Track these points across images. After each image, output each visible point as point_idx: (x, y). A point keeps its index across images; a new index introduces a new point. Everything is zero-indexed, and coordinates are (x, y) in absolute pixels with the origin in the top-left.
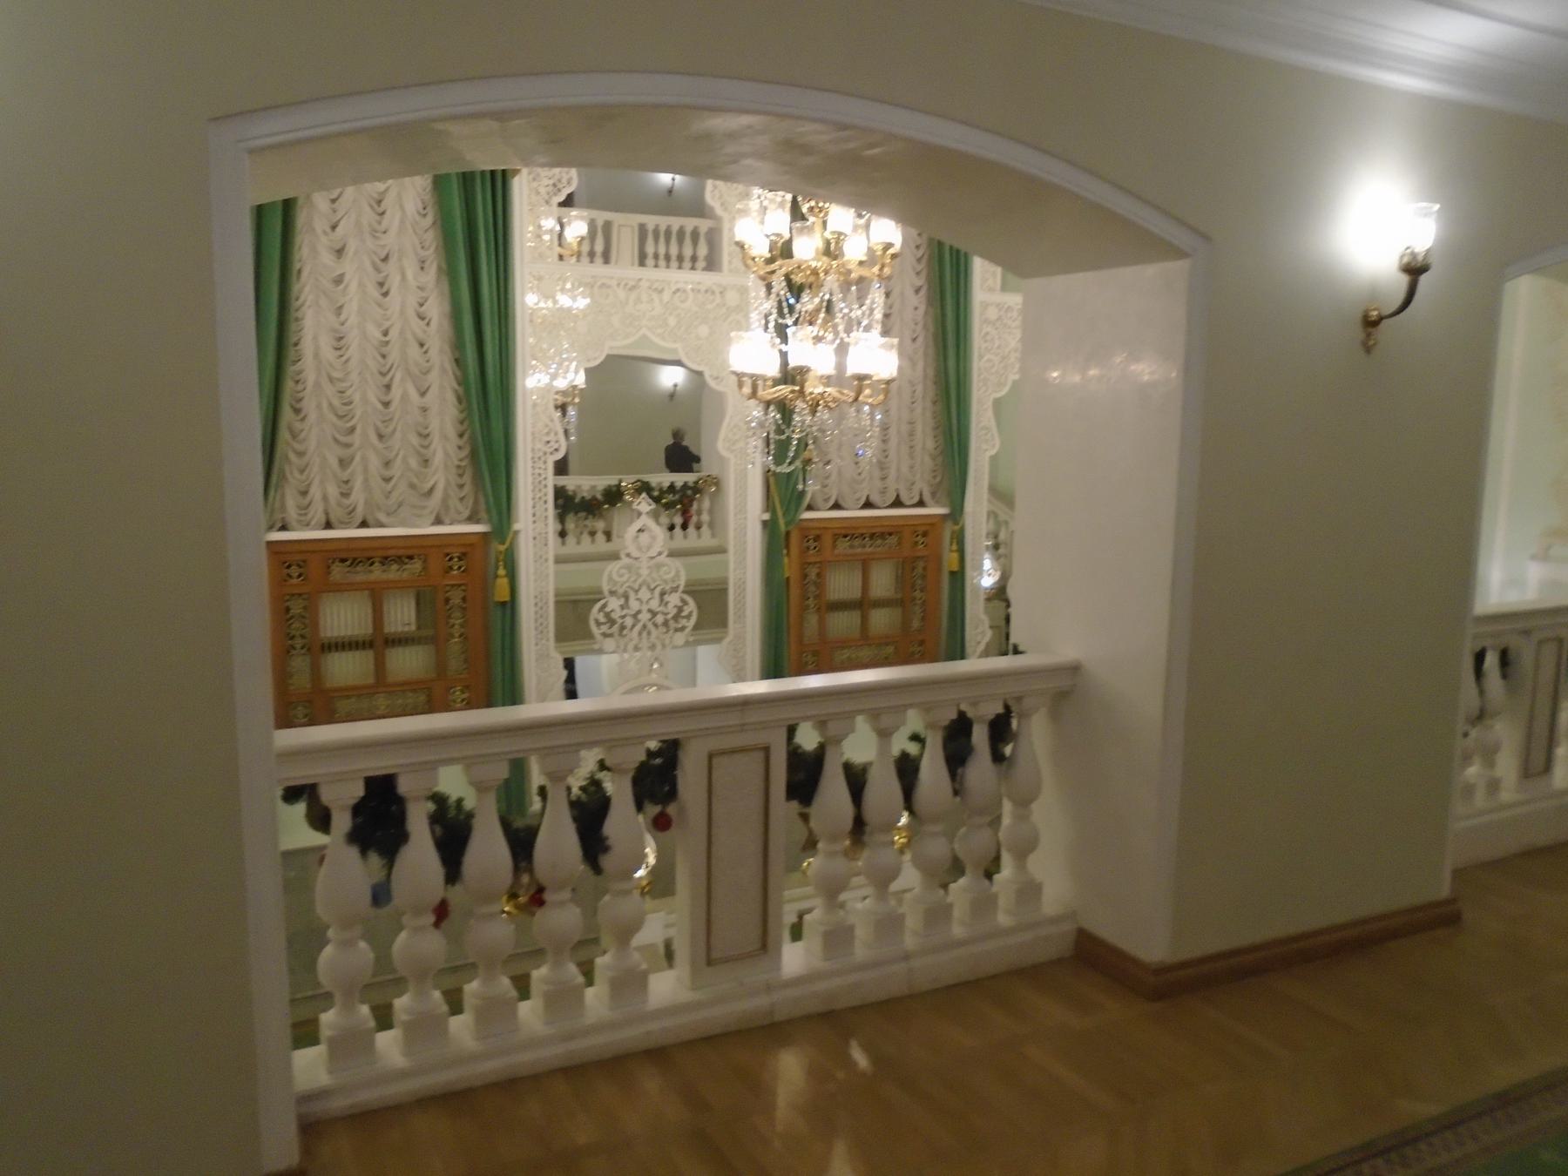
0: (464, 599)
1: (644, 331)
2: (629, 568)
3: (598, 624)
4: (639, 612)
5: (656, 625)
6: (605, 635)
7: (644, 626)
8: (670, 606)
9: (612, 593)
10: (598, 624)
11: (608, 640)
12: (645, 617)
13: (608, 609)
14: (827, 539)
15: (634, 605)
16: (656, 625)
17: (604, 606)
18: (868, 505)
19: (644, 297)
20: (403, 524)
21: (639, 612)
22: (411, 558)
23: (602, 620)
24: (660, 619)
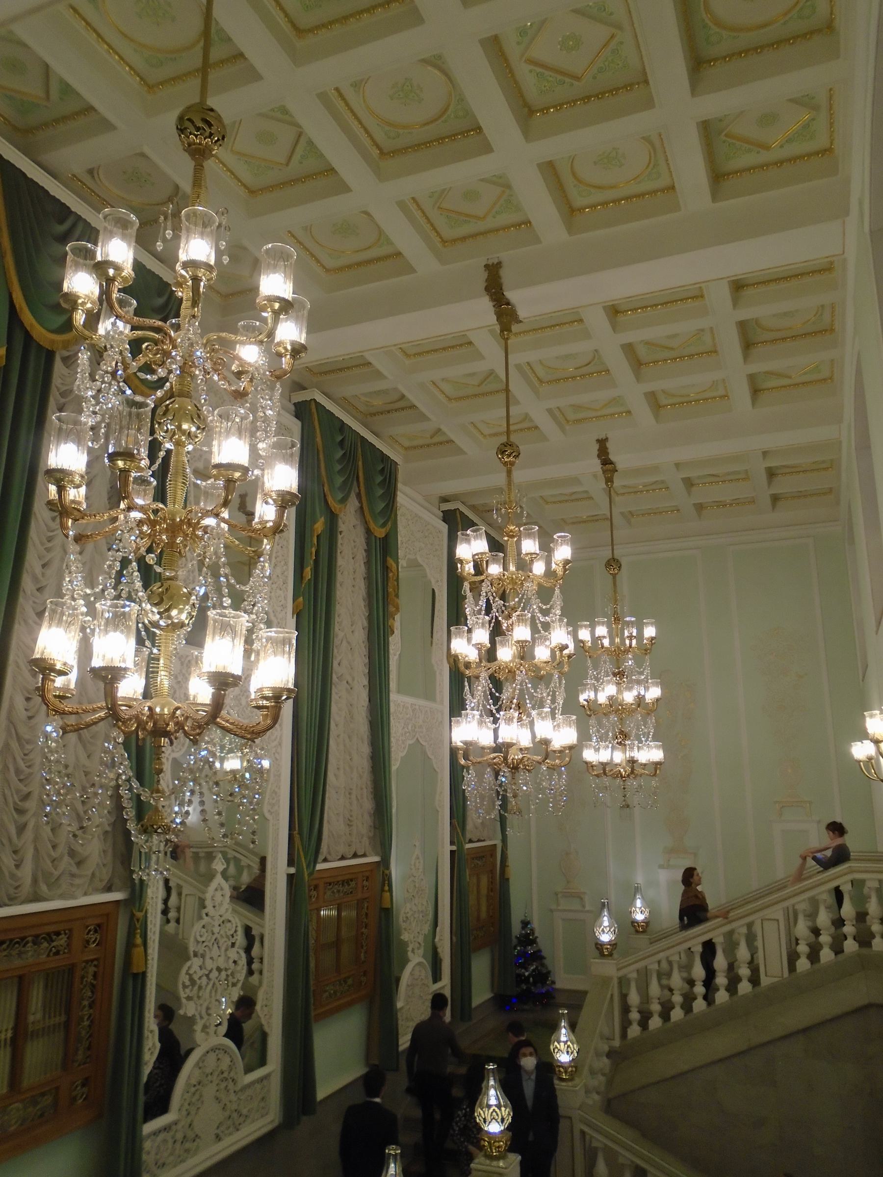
0: (95, 975)
4: (211, 971)
6: (189, 998)
7: (214, 984)
9: (196, 955)
10: (185, 987)
11: (191, 1003)
15: (209, 964)
17: (189, 968)
18: (343, 858)
20: (62, 897)
22: (58, 934)
23: (188, 983)
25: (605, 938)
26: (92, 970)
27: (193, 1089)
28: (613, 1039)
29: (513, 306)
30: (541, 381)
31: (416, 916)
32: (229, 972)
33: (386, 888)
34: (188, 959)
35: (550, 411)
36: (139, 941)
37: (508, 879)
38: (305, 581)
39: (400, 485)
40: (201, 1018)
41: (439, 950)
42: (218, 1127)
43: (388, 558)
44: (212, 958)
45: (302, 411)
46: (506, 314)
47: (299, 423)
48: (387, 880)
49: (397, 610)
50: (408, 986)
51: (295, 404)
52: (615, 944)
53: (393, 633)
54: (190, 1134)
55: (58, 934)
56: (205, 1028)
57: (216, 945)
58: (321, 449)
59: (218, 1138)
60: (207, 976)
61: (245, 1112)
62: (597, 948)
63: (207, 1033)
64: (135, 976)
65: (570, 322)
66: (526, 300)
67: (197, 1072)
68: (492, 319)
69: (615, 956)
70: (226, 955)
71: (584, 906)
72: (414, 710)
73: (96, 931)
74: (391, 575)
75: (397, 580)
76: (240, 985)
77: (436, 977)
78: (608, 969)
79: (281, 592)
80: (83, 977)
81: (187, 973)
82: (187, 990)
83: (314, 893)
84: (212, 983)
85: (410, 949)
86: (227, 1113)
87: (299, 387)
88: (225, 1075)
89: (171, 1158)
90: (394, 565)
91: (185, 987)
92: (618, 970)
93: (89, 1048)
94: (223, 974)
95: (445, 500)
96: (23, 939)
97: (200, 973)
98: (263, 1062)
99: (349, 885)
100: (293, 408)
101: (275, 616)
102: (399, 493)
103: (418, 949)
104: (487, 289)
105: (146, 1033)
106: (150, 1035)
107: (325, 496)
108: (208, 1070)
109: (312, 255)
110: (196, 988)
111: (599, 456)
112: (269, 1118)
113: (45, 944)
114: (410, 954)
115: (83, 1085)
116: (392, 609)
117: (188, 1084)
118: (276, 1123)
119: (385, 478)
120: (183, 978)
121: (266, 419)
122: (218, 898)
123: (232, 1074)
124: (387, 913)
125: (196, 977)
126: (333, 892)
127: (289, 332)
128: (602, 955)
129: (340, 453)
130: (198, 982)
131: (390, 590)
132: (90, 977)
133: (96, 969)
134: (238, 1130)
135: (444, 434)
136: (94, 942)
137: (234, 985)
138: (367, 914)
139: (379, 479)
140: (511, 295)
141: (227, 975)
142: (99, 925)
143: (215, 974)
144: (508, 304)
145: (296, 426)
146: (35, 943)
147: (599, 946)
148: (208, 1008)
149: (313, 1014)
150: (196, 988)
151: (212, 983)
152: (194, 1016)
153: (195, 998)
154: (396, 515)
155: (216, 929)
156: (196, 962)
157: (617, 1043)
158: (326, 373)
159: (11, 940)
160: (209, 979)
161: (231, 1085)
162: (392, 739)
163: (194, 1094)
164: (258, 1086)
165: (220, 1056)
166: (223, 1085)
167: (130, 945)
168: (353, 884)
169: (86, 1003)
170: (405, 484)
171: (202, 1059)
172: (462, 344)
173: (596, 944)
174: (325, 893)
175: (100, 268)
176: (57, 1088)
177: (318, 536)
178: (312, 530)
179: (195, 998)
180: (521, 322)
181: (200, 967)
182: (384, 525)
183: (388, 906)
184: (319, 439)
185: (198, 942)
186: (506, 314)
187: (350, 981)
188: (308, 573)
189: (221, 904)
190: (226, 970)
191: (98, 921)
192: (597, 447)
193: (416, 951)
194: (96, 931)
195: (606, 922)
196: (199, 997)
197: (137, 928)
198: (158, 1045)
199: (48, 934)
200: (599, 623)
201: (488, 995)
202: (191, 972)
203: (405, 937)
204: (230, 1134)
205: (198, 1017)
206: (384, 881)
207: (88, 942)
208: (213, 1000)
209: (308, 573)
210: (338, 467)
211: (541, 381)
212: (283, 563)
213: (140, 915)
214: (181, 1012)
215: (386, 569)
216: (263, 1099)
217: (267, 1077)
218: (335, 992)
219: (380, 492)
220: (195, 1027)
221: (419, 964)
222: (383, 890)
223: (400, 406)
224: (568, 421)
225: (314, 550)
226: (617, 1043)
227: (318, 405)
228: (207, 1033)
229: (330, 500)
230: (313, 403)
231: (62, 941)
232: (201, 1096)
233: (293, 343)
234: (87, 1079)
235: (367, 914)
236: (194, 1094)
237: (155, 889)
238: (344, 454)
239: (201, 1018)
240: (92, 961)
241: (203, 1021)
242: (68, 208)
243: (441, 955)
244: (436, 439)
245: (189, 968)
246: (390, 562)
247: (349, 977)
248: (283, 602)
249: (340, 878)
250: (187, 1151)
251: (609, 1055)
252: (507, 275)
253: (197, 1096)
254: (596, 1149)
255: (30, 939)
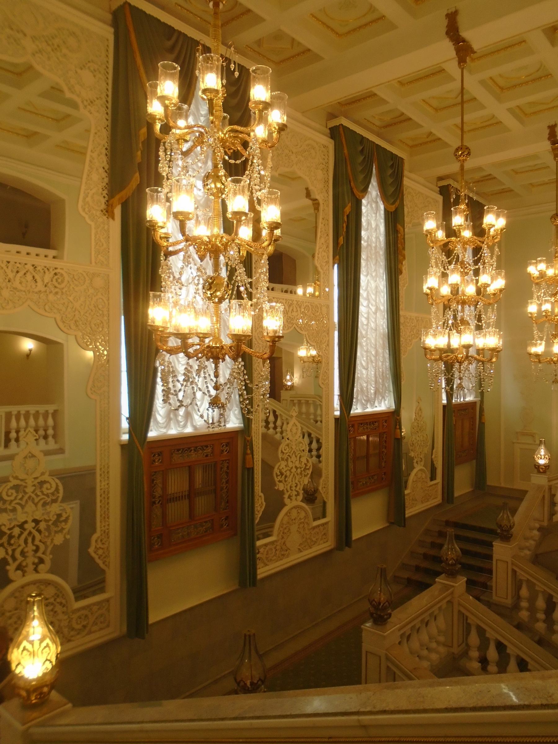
0: (228, 467)
1: (295, 325)
2: (288, 445)
3: (277, 476)
4: (292, 468)
5: (297, 474)
6: (280, 481)
7: (294, 475)
8: (303, 464)
9: (283, 459)
12: (294, 470)
13: (281, 468)
14: (356, 426)
15: (290, 465)
16: (297, 474)
17: (279, 466)
19: (295, 310)
21: (292, 468)
22: (207, 447)
23: (279, 474)
24: (299, 470)
25: (542, 462)
26: (226, 465)
27: (285, 526)
28: (543, 521)
29: (467, 42)
30: (502, 89)
31: (419, 443)
32: (302, 469)
33: (398, 427)
34: (279, 461)
35: (510, 110)
36: (249, 451)
37: (484, 423)
38: (340, 246)
39: (406, 173)
40: (287, 491)
41: (435, 463)
42: (299, 546)
43: (398, 224)
44: (292, 462)
45: (335, 133)
46: (463, 50)
47: (332, 142)
48: (398, 423)
49: (404, 258)
50: (413, 481)
51: (330, 129)
52: (549, 466)
53: (401, 273)
54: (284, 547)
55: (207, 447)
56: (290, 497)
57: (294, 455)
58: (347, 158)
59: (300, 551)
60: (290, 470)
61: (314, 539)
62: (536, 468)
63: (291, 500)
64: (249, 469)
65: (515, 46)
66: (477, 36)
67: (286, 519)
68: (453, 53)
69: (548, 473)
70: (300, 461)
71: (535, 441)
72: (417, 321)
73: (227, 446)
74: (399, 235)
75: (404, 239)
76: (309, 476)
77: (433, 478)
78: (541, 480)
79: (325, 254)
80: (222, 468)
81: (278, 468)
82: (279, 477)
83: (352, 429)
84: (292, 475)
85: (415, 461)
86: (304, 539)
87: (332, 116)
88: (303, 520)
89: (275, 557)
90: (402, 229)
91: (277, 476)
92: (549, 481)
93: (227, 502)
94: (299, 470)
95: (440, 179)
96: (189, 448)
97: (285, 469)
98: (324, 516)
99: (374, 425)
100: (329, 131)
101: (322, 268)
102: (405, 179)
103: (421, 461)
104: (447, 33)
105: (256, 498)
106: (260, 499)
107: (352, 189)
108: (293, 518)
109: (328, 27)
110: (284, 476)
111: (549, 139)
112: (329, 543)
113: (201, 451)
114: (415, 465)
115: (226, 519)
116: (401, 258)
117: (282, 524)
118: (332, 547)
119: (394, 171)
120: (276, 471)
121: (261, 178)
122: (294, 430)
123: (306, 521)
124: (399, 440)
125: (283, 471)
126: (364, 429)
127: (276, 117)
128: (539, 472)
129: (361, 158)
130: (285, 473)
131: (399, 245)
132: (225, 469)
133: (227, 464)
134: (311, 548)
135: (434, 135)
136: (226, 451)
137: (305, 476)
138: (386, 441)
139: (390, 171)
140: (465, 34)
141: (301, 471)
142: (228, 443)
143: (294, 470)
144: (464, 41)
145: (330, 144)
146: (195, 451)
147: (538, 467)
148: (291, 487)
149: (351, 494)
150: (284, 476)
151: (292, 475)
152: (283, 490)
153: (283, 481)
154: (403, 195)
155: (294, 447)
156: (283, 464)
157: (545, 523)
158: (349, 104)
159: (183, 449)
160: (291, 472)
161: (306, 526)
162: (401, 339)
163: (285, 528)
164: (321, 528)
165: (299, 511)
166: (301, 526)
167: (245, 454)
168: (376, 424)
169: (224, 481)
170: (410, 171)
171: (289, 512)
172: (438, 72)
173: (535, 465)
174: (358, 429)
175: (162, 99)
176: (212, 520)
177: (348, 216)
178: (343, 212)
179: (283, 481)
180: (475, 52)
181: (286, 466)
182: (393, 203)
183: (399, 437)
184: (346, 151)
185: (283, 453)
186: (463, 50)
187: (376, 477)
188: (341, 240)
189: (296, 433)
190: (301, 468)
191: (227, 441)
192: (547, 131)
193: (419, 463)
194: (227, 446)
195: (542, 452)
196: (285, 481)
197: (249, 445)
198: (264, 503)
199: (202, 447)
200: (540, 261)
201: (468, 489)
202: (281, 468)
203: (412, 454)
204: (307, 549)
205: (285, 491)
206: (396, 423)
207: (223, 451)
208: (294, 483)
209: (341, 240)
210: (360, 168)
211: (502, 89)
212: (325, 235)
213: (249, 438)
214: (276, 488)
215: (396, 231)
216: (324, 534)
217: (327, 523)
218: (366, 483)
219: (390, 181)
220: (284, 496)
221: (421, 470)
222: (396, 428)
223: (402, 120)
224: (526, 115)
225: (345, 225)
226: (545, 523)
227: (345, 128)
228: (291, 500)
229: (355, 191)
230: (341, 126)
231: (209, 450)
232: (289, 530)
233: (278, 124)
234: (227, 517)
235: (386, 441)
236: (285, 528)
237: (257, 425)
238: (365, 158)
239: (287, 491)
240: (226, 460)
241: (289, 493)
242: (173, 28)
243: (436, 465)
244: (431, 138)
245: (279, 466)
246: (399, 227)
247: (374, 475)
248: (327, 260)
249: (367, 421)
250: (283, 555)
251: (539, 530)
252: (462, 21)
253: (287, 530)
254: (521, 581)
255: (193, 448)
